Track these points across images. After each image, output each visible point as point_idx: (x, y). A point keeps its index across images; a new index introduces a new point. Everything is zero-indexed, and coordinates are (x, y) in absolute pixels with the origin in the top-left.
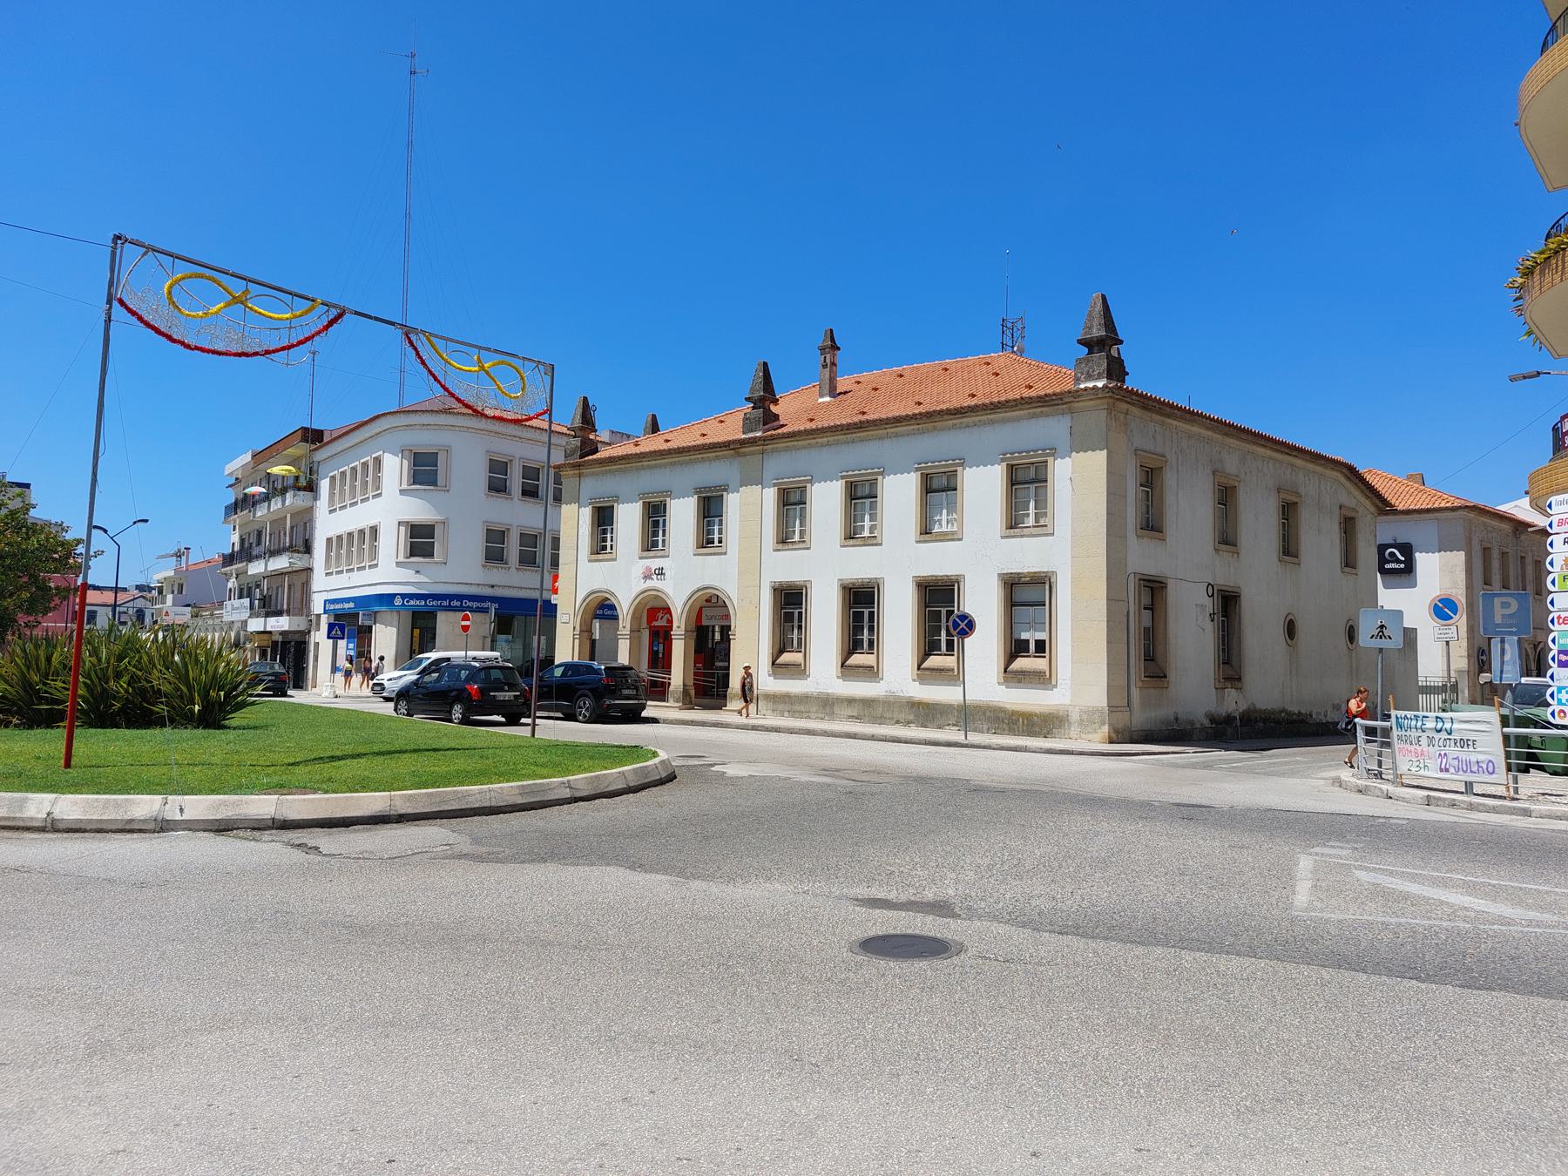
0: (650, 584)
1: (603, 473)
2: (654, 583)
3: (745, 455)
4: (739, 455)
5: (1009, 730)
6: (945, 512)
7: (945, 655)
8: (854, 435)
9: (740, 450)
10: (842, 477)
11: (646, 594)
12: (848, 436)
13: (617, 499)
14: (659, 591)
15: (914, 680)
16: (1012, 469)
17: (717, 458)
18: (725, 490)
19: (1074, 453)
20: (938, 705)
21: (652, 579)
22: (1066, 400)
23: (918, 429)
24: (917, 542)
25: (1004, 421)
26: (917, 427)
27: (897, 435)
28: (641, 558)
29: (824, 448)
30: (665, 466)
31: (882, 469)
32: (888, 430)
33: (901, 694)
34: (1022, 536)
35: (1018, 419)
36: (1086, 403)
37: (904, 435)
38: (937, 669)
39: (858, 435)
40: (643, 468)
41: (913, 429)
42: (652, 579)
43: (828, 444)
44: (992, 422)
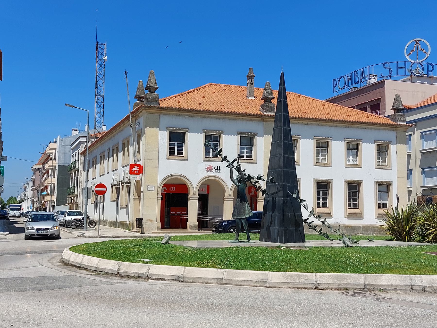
0: (210, 174)
1: (176, 115)
2: (214, 173)
3: (267, 121)
4: (264, 121)
5: (380, 234)
6: (351, 157)
7: (353, 208)
8: (320, 123)
9: (265, 119)
10: (314, 139)
11: (208, 179)
12: (317, 123)
13: (187, 130)
14: (216, 177)
15: (345, 218)
16: (378, 146)
17: (251, 120)
18: (256, 135)
19: (397, 144)
20: (355, 226)
21: (212, 172)
22: (398, 127)
23: (345, 126)
24: (345, 167)
25: (375, 129)
26: (345, 125)
27: (337, 126)
28: (204, 161)
29: (306, 126)
30: (219, 118)
31: (332, 138)
32: (334, 124)
33: (340, 223)
34: (382, 169)
35: (380, 129)
36: (402, 129)
37: (339, 127)
38: (355, 214)
39: (321, 123)
40: (205, 117)
41: (343, 125)
42: (212, 172)
43: (307, 124)
44: (371, 129)
